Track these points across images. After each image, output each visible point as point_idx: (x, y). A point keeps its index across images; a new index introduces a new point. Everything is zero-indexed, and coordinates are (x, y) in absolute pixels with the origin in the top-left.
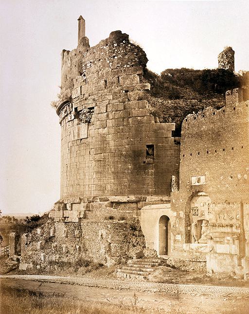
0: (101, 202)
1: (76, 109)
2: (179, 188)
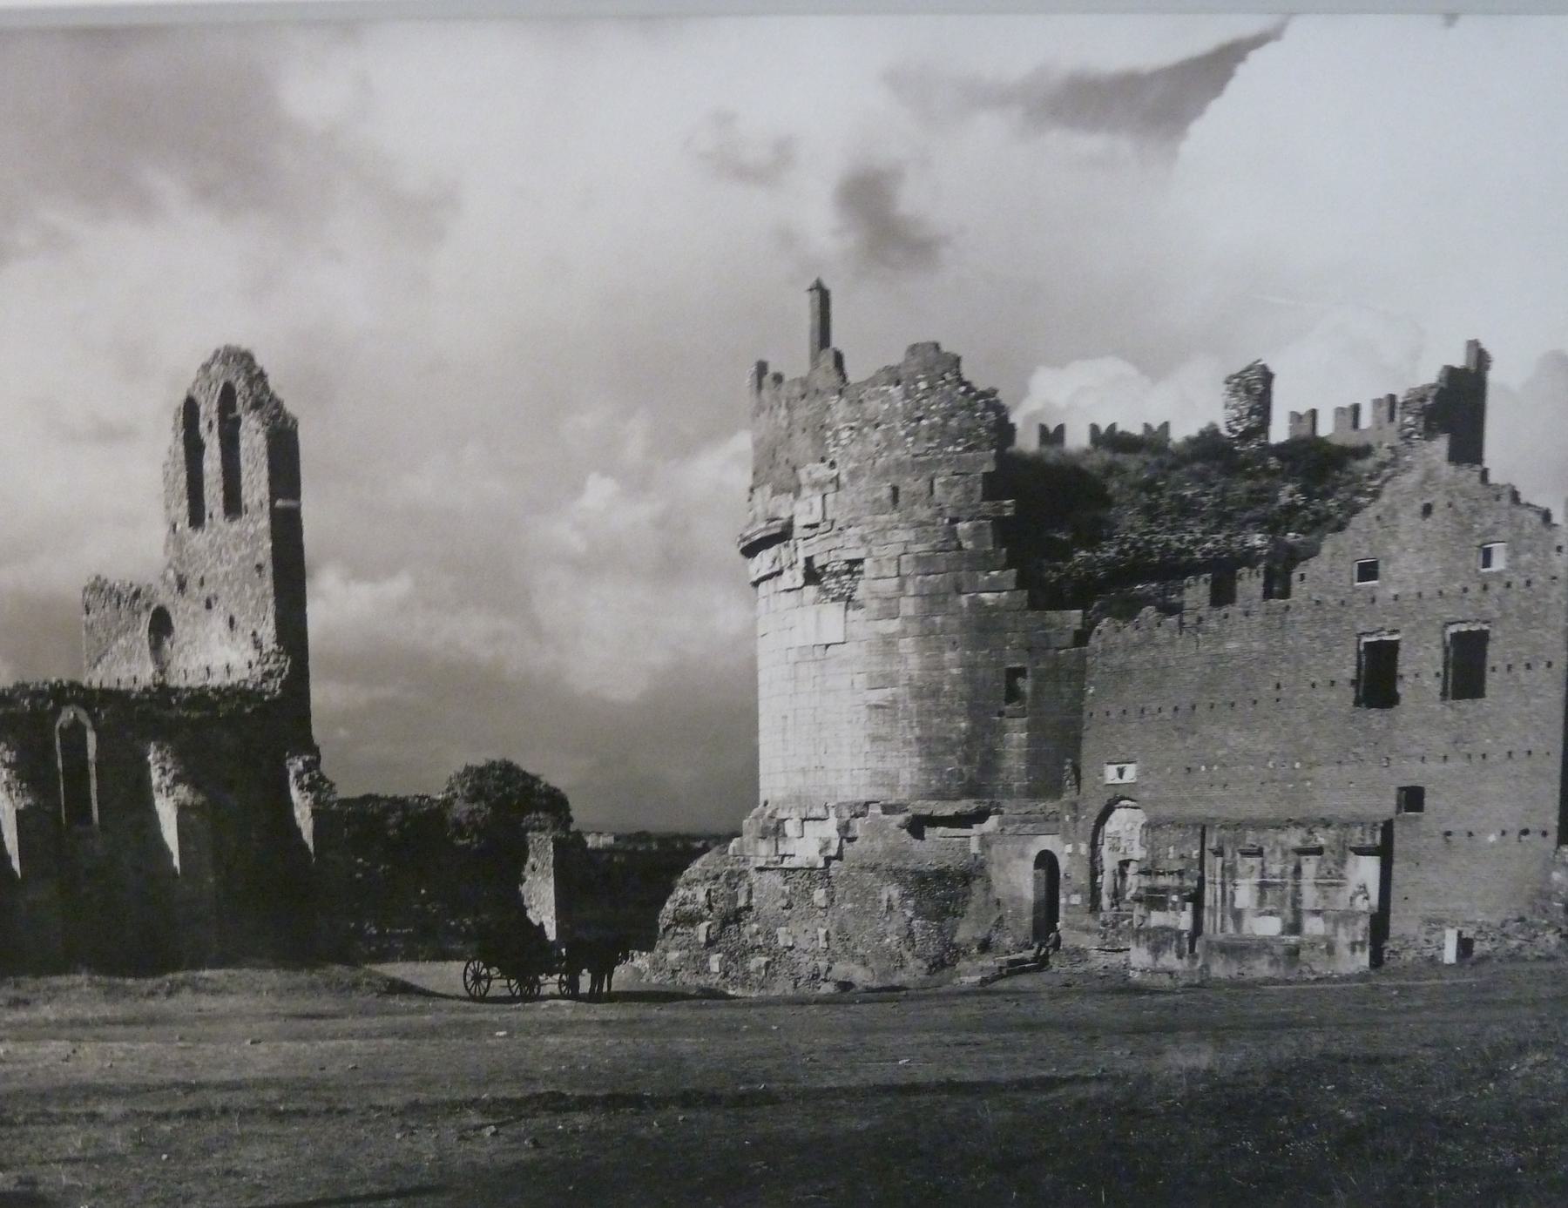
0: (887, 817)
1: (809, 560)
2: (1079, 789)
